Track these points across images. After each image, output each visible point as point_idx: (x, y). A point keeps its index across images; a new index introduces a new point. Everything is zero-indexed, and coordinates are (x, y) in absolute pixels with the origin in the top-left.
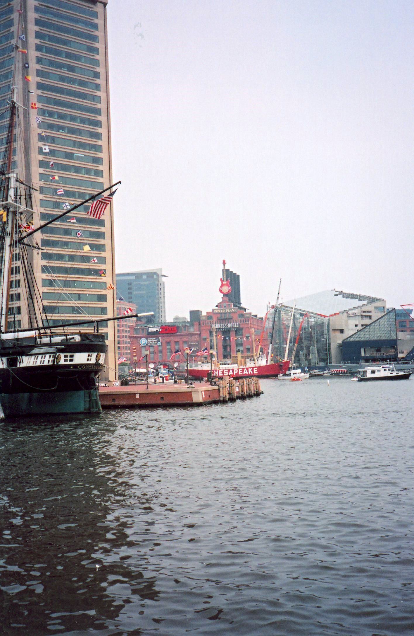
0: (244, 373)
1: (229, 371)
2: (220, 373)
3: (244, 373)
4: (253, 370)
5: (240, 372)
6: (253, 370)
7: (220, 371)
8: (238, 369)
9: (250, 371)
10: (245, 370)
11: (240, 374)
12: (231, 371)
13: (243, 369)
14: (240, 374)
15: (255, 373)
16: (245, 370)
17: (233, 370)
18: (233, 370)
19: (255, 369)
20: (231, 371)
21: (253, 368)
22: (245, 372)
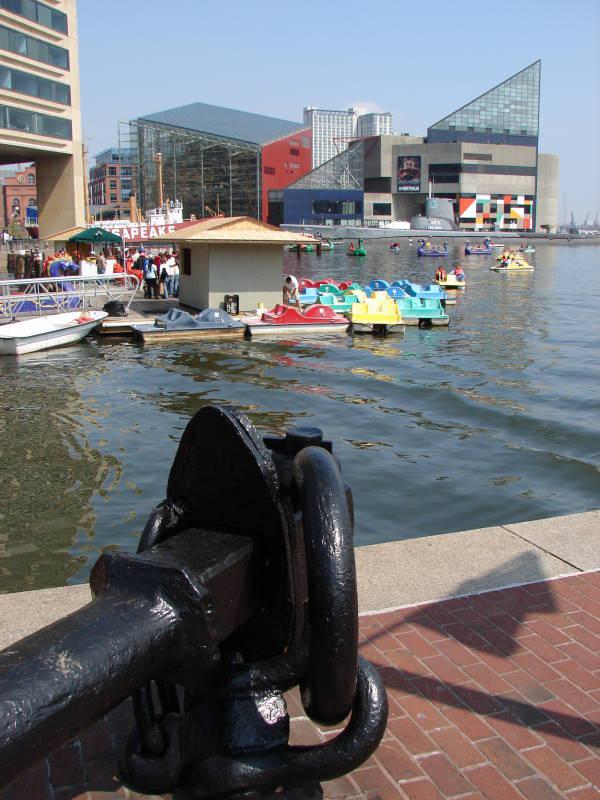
0: (151, 235)
3: (151, 235)
5: (143, 233)
6: (166, 231)
8: (139, 228)
9: (162, 231)
10: (153, 229)
13: (149, 228)
14: (143, 237)
16: (153, 229)
17: (129, 230)
18: (129, 230)
19: (170, 228)
20: (126, 231)
21: (167, 226)
22: (153, 234)
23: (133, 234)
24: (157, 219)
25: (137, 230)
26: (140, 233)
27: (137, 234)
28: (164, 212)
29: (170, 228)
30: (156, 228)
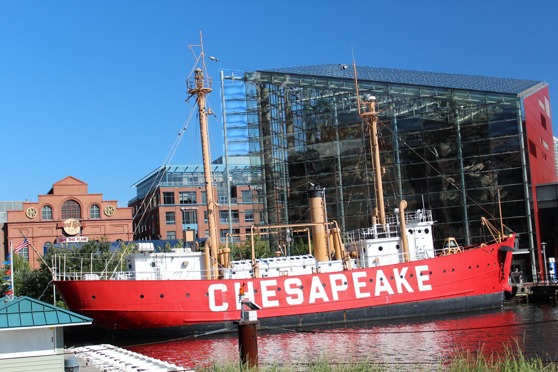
1: (306, 282)
2: (265, 294)
4: (411, 276)
5: (358, 285)
6: (411, 276)
7: (264, 284)
9: (401, 281)
10: (380, 274)
11: (359, 295)
12: (316, 282)
13: (372, 272)
14: (359, 295)
15: (422, 288)
16: (380, 274)
17: (325, 279)
18: (325, 279)
19: (419, 269)
20: (316, 282)
23: (335, 289)
24: (381, 251)
25: (344, 278)
26: (350, 282)
27: (344, 288)
28: (397, 232)
29: (419, 269)
30: (388, 270)
